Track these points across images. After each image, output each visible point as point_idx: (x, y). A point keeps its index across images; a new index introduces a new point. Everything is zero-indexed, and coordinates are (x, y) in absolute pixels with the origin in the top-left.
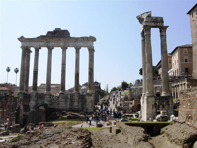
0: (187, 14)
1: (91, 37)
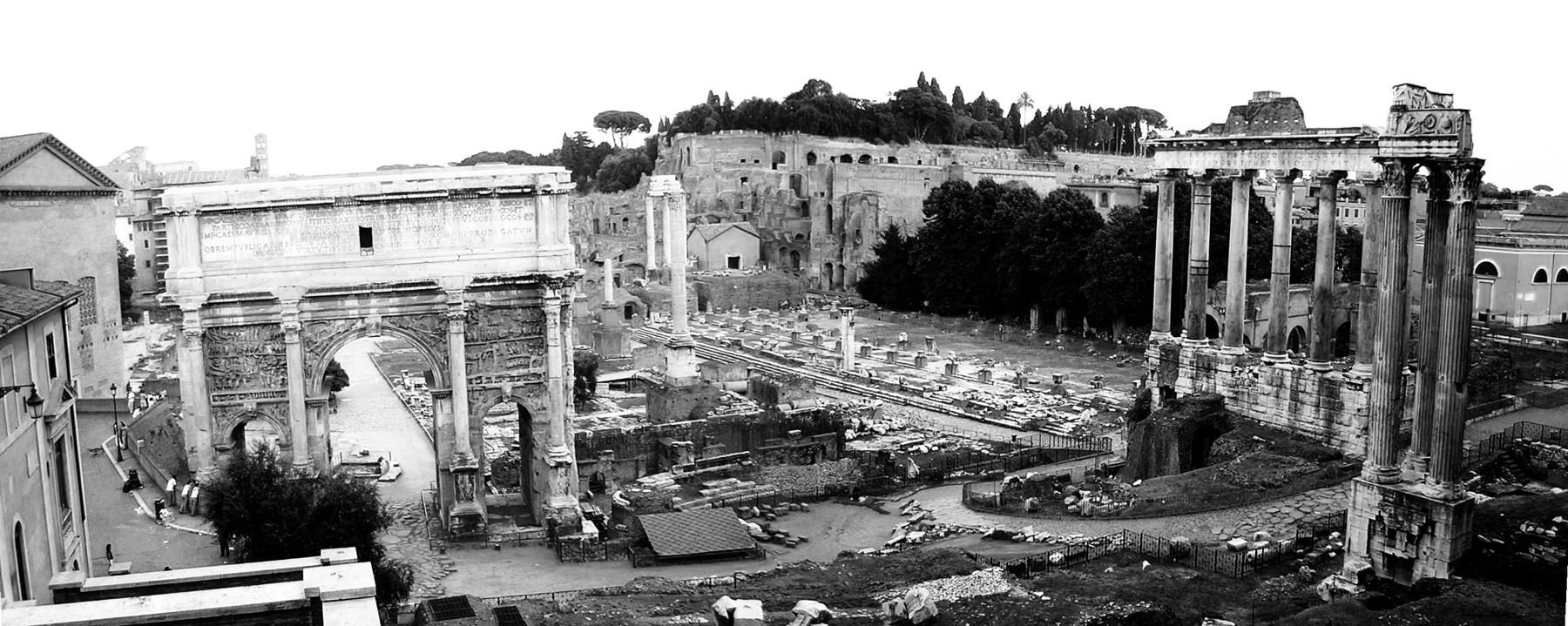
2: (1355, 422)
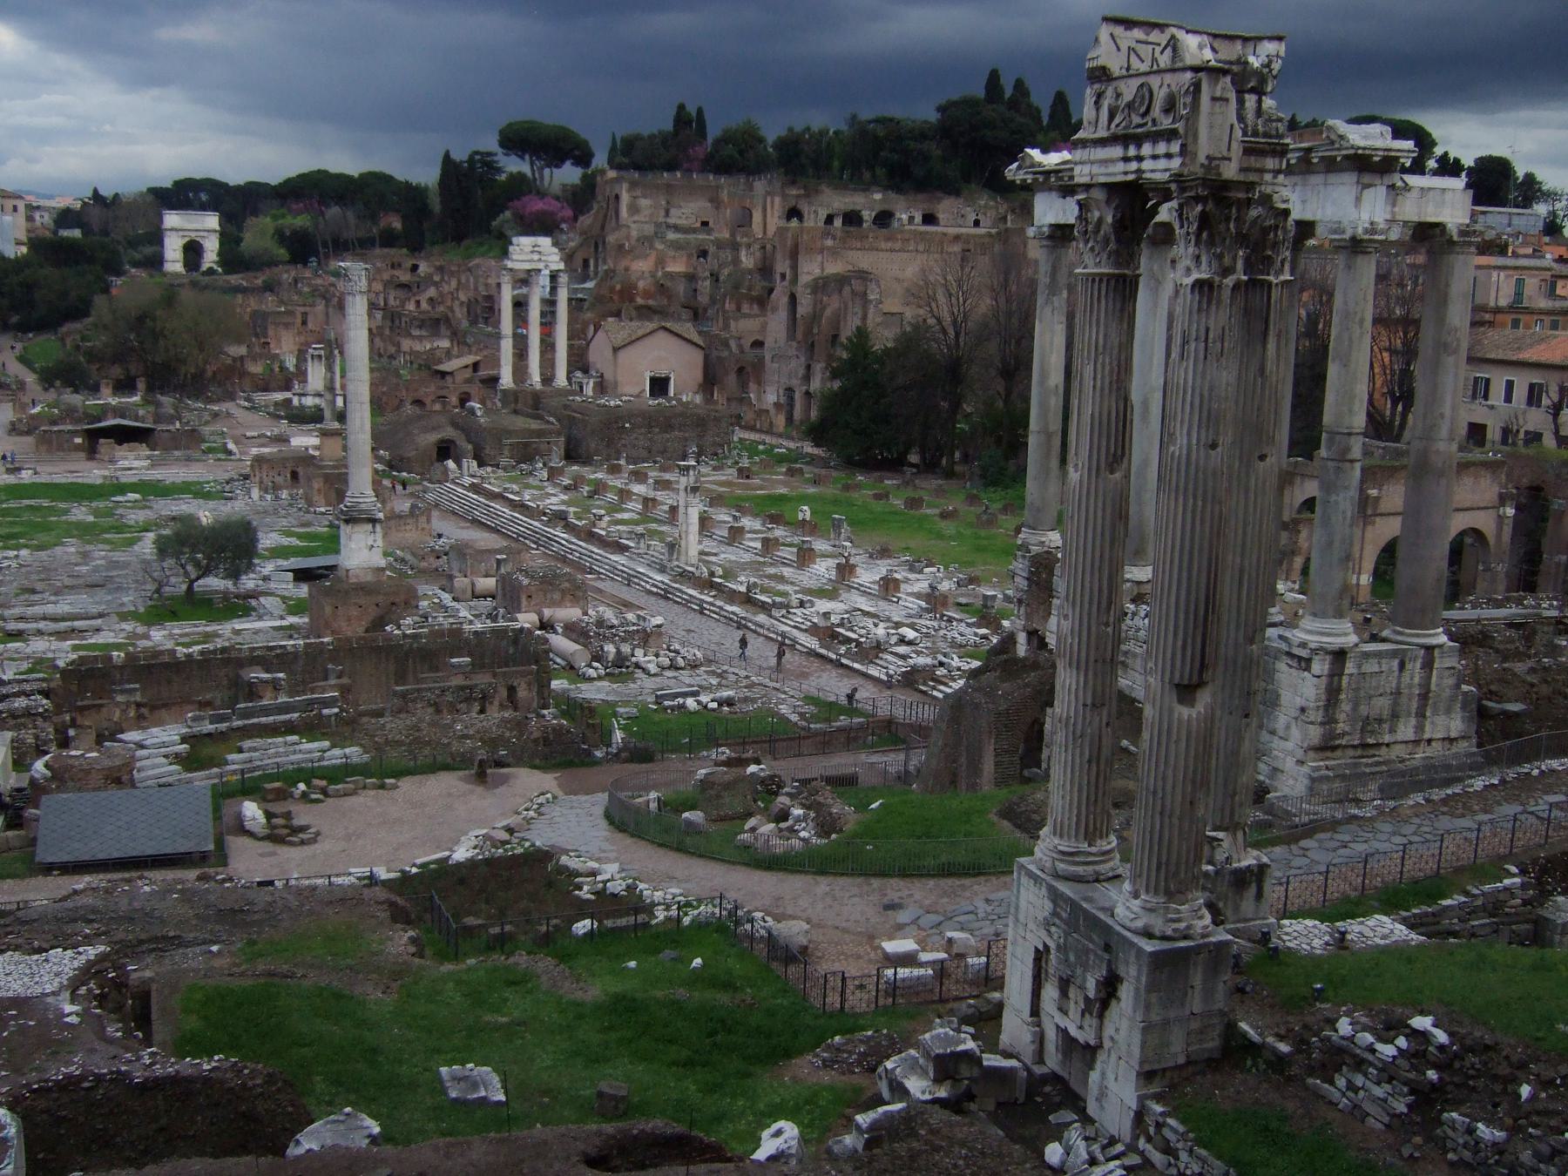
2: (1295, 733)
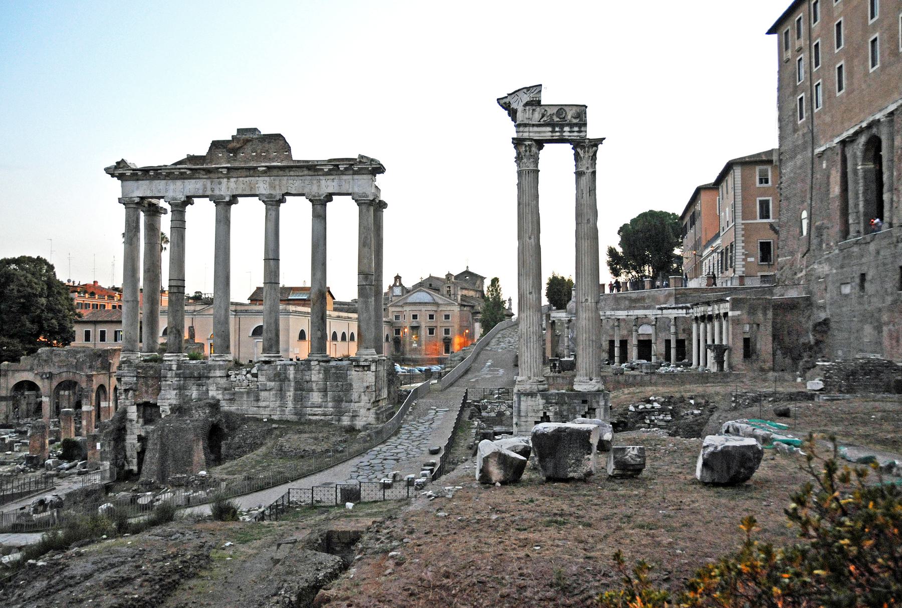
0: (768, 33)
1: (364, 160)
2: (365, 398)
